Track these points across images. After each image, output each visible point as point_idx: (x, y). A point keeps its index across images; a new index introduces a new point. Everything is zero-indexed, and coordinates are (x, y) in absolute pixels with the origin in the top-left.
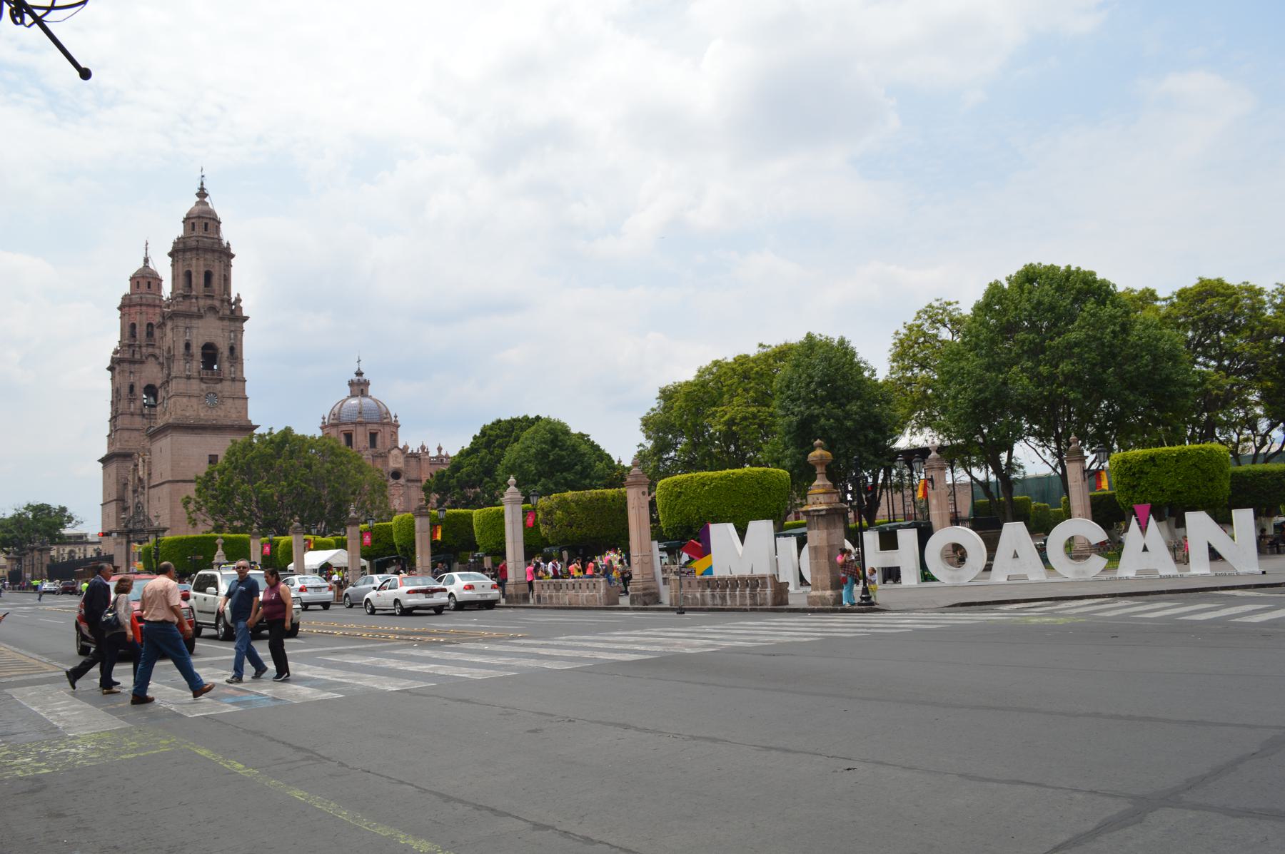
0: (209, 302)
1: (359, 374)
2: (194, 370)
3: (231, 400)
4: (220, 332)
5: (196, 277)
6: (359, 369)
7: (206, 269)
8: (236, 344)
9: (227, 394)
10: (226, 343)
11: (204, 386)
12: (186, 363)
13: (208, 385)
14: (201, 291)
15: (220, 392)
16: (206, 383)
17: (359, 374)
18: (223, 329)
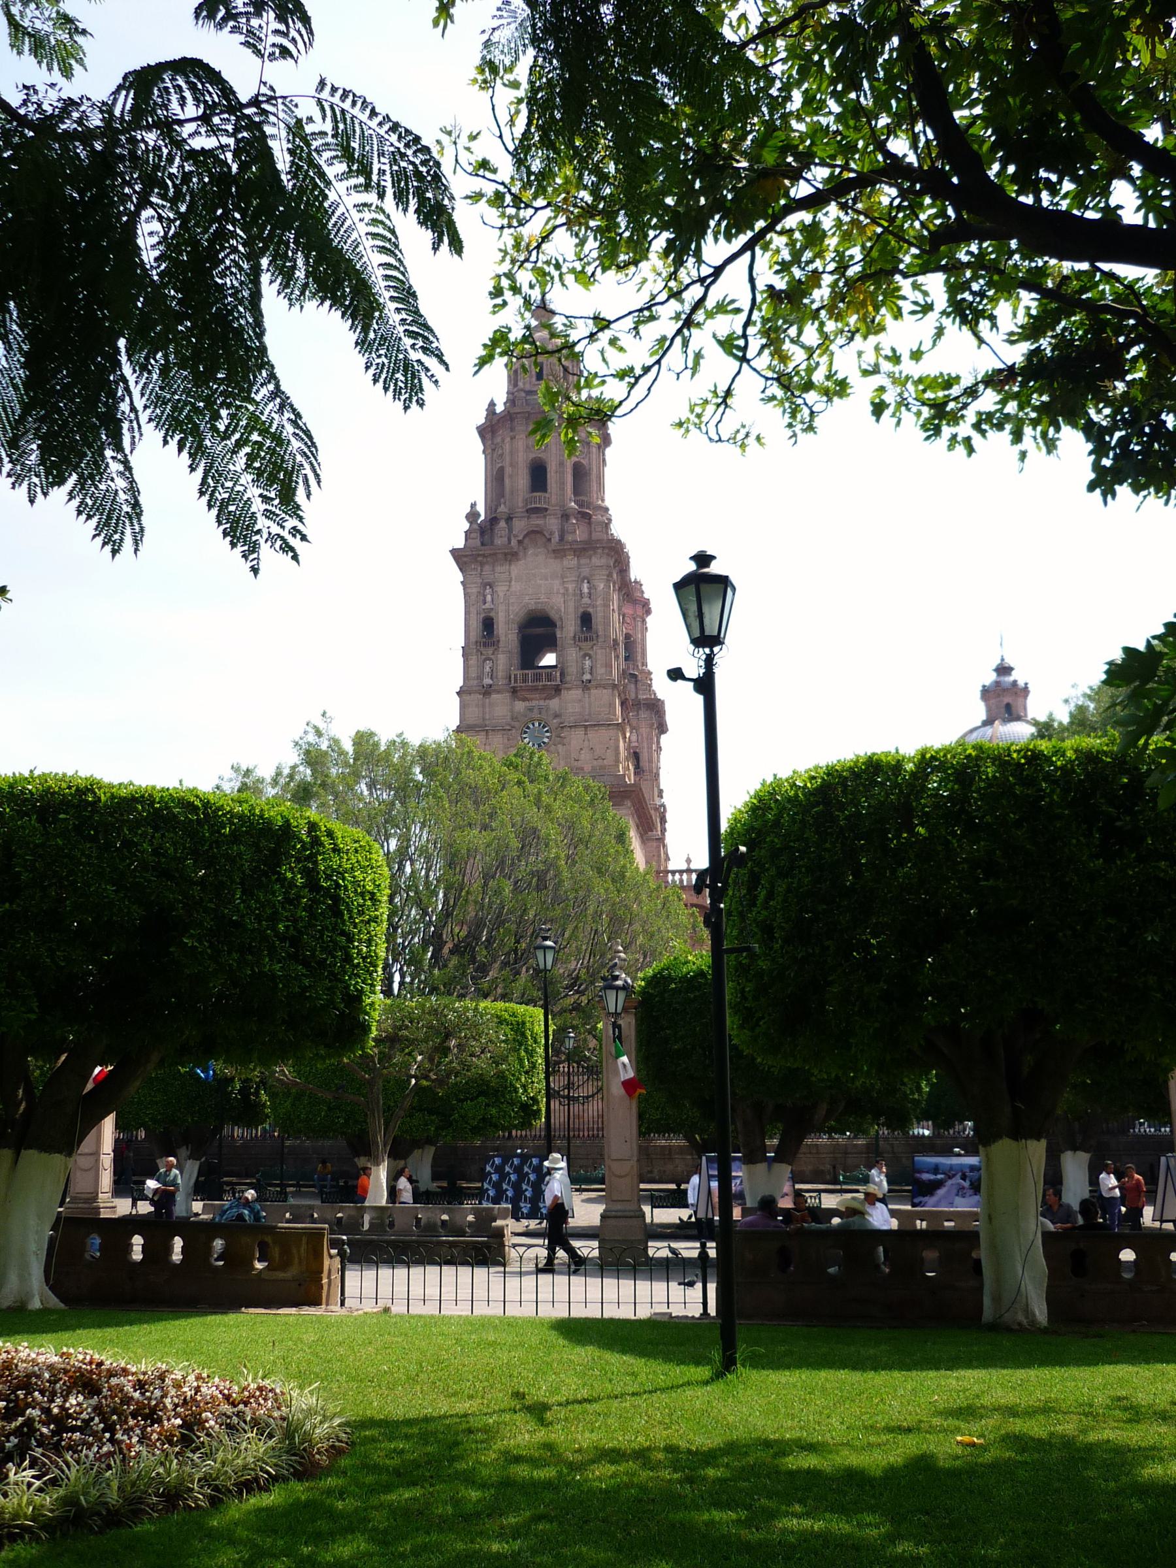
0: (537, 521)
1: (1003, 670)
2: (500, 674)
3: (580, 732)
4: (556, 584)
5: (511, 476)
6: (1003, 660)
7: (532, 456)
8: (594, 606)
9: (569, 720)
10: (571, 609)
11: (520, 706)
12: (485, 660)
13: (527, 704)
14: (520, 505)
15: (556, 716)
16: (524, 699)
17: (1003, 670)
18: (563, 577)
